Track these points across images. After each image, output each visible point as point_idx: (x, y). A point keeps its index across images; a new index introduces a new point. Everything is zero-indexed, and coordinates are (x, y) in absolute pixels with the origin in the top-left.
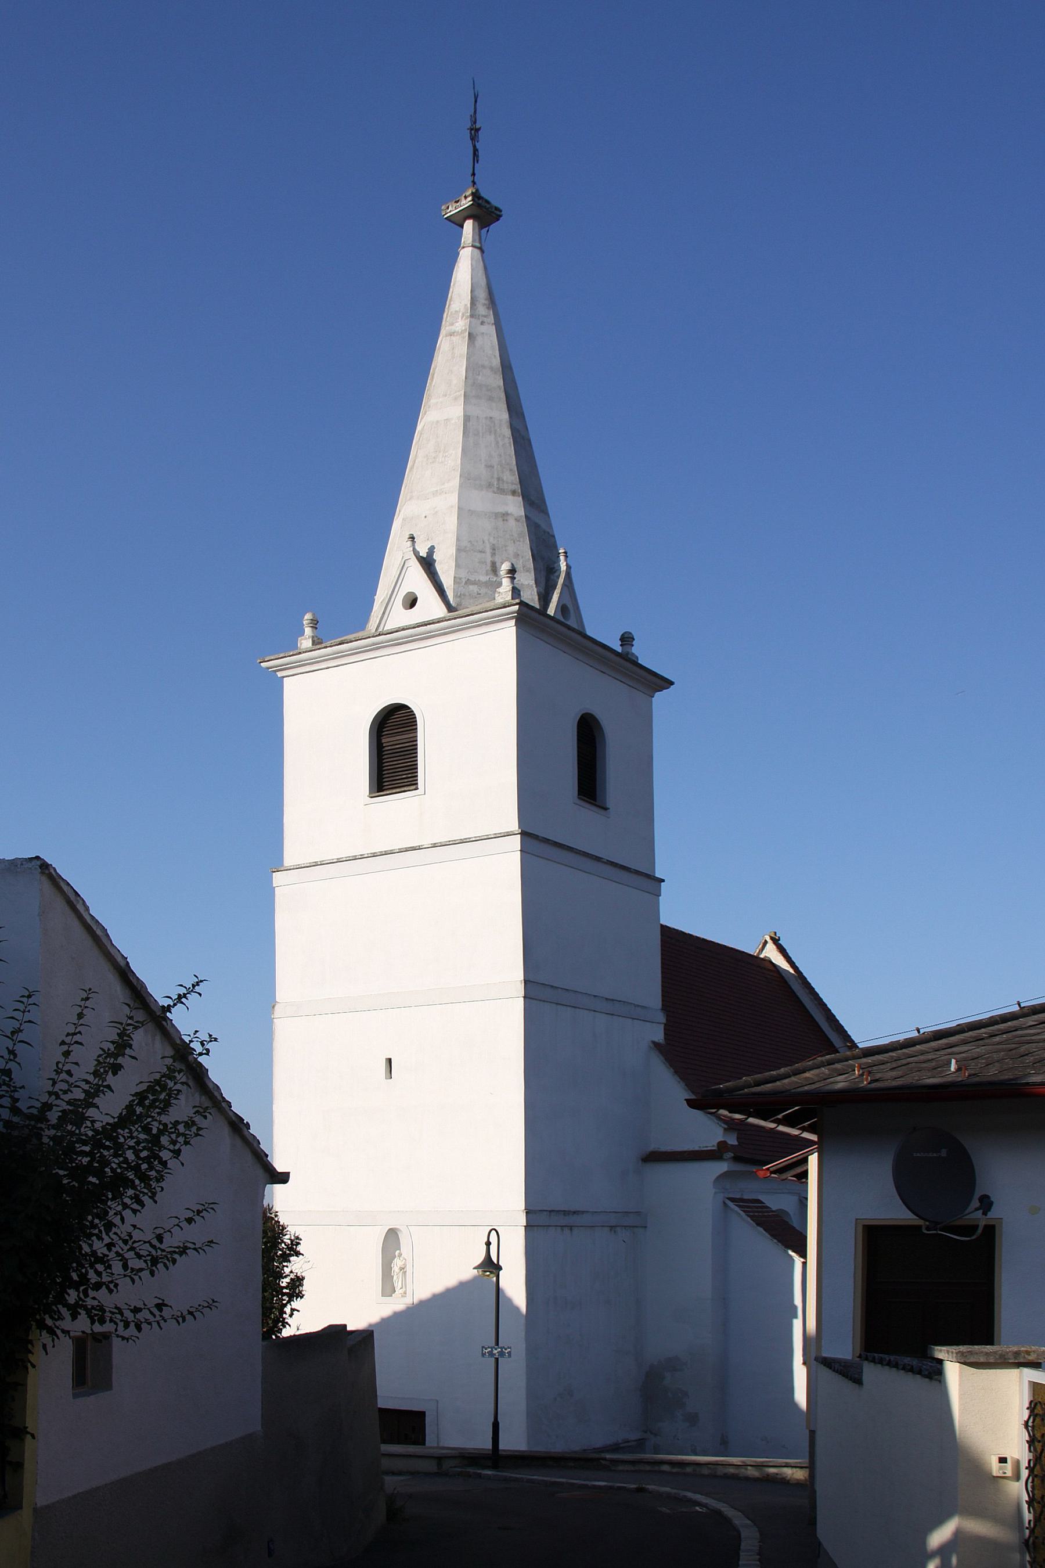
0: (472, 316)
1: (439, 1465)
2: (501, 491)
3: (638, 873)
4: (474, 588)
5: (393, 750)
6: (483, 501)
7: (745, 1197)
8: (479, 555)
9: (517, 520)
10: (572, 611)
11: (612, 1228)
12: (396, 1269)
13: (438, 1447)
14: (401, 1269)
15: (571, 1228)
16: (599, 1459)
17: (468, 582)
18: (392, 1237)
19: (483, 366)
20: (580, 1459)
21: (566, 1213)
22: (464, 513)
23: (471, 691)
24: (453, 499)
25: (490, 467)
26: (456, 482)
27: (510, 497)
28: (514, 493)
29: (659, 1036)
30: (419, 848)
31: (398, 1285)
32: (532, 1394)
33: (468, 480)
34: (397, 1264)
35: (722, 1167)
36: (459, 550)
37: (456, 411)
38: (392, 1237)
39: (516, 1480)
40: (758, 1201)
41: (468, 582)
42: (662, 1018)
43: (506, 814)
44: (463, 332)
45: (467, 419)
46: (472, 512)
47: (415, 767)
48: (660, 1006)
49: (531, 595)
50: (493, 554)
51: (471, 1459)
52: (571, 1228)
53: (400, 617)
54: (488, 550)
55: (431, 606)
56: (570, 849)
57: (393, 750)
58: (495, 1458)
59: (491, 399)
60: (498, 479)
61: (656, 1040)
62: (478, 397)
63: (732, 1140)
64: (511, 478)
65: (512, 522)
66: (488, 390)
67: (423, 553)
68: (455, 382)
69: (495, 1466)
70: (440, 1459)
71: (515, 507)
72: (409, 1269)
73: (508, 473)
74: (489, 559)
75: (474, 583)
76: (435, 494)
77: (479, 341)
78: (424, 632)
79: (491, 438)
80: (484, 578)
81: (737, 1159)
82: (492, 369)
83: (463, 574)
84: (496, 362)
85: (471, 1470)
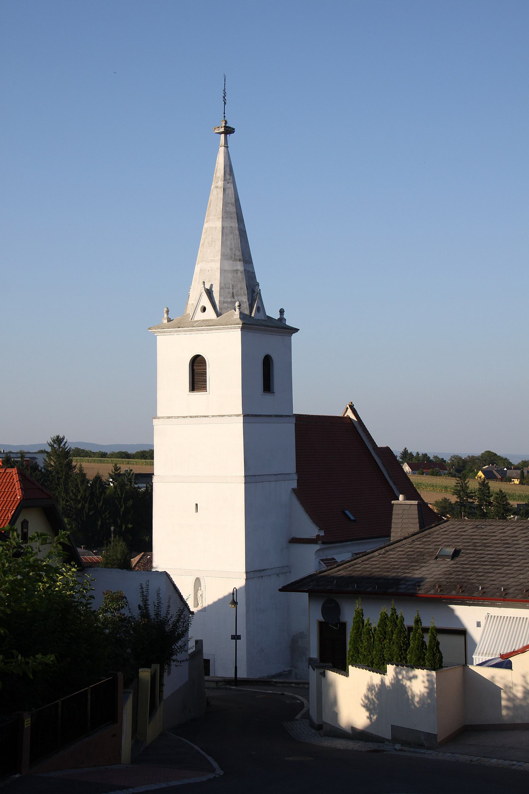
0: (224, 180)
1: (217, 684)
2: (235, 260)
3: (286, 416)
4: (226, 305)
5: (198, 373)
6: (229, 265)
7: (328, 558)
8: (228, 290)
9: (241, 272)
10: (261, 308)
11: (278, 575)
12: (199, 595)
13: (215, 677)
14: (201, 595)
15: (262, 577)
16: (271, 681)
17: (224, 302)
18: (198, 580)
19: (229, 203)
20: (264, 682)
21: (260, 571)
22: (223, 271)
23: (225, 350)
24: (218, 265)
25: (231, 249)
26: (219, 257)
27: (239, 262)
28: (240, 260)
29: (294, 485)
30: (208, 416)
31: (200, 602)
32: (248, 652)
33: (224, 256)
34: (200, 593)
35: (317, 547)
36: (220, 288)
37: (219, 224)
38: (198, 580)
39: (243, 690)
40: (334, 559)
41: (224, 302)
42: (296, 477)
43: (239, 409)
44: (221, 187)
45: (223, 228)
46: (225, 271)
47: (205, 381)
48: (295, 471)
49: (247, 312)
50: (233, 289)
51: (228, 682)
52: (262, 577)
53: (200, 316)
54: (231, 287)
55: (210, 314)
56: (260, 416)
57: (198, 373)
58: (236, 681)
59: (231, 218)
60: (234, 255)
61: (294, 487)
62: (227, 218)
63: (322, 534)
64: (239, 253)
65: (239, 274)
66: (230, 214)
67: (208, 287)
68: (218, 210)
69: (236, 685)
70: (217, 682)
71: (240, 266)
72: (204, 595)
73: (238, 251)
74: (231, 291)
75: (227, 302)
76: (212, 261)
77: (227, 192)
78: (207, 324)
79: (231, 236)
80: (229, 300)
81: (323, 543)
82: (232, 204)
83: (222, 299)
84: (233, 200)
85: (228, 686)
